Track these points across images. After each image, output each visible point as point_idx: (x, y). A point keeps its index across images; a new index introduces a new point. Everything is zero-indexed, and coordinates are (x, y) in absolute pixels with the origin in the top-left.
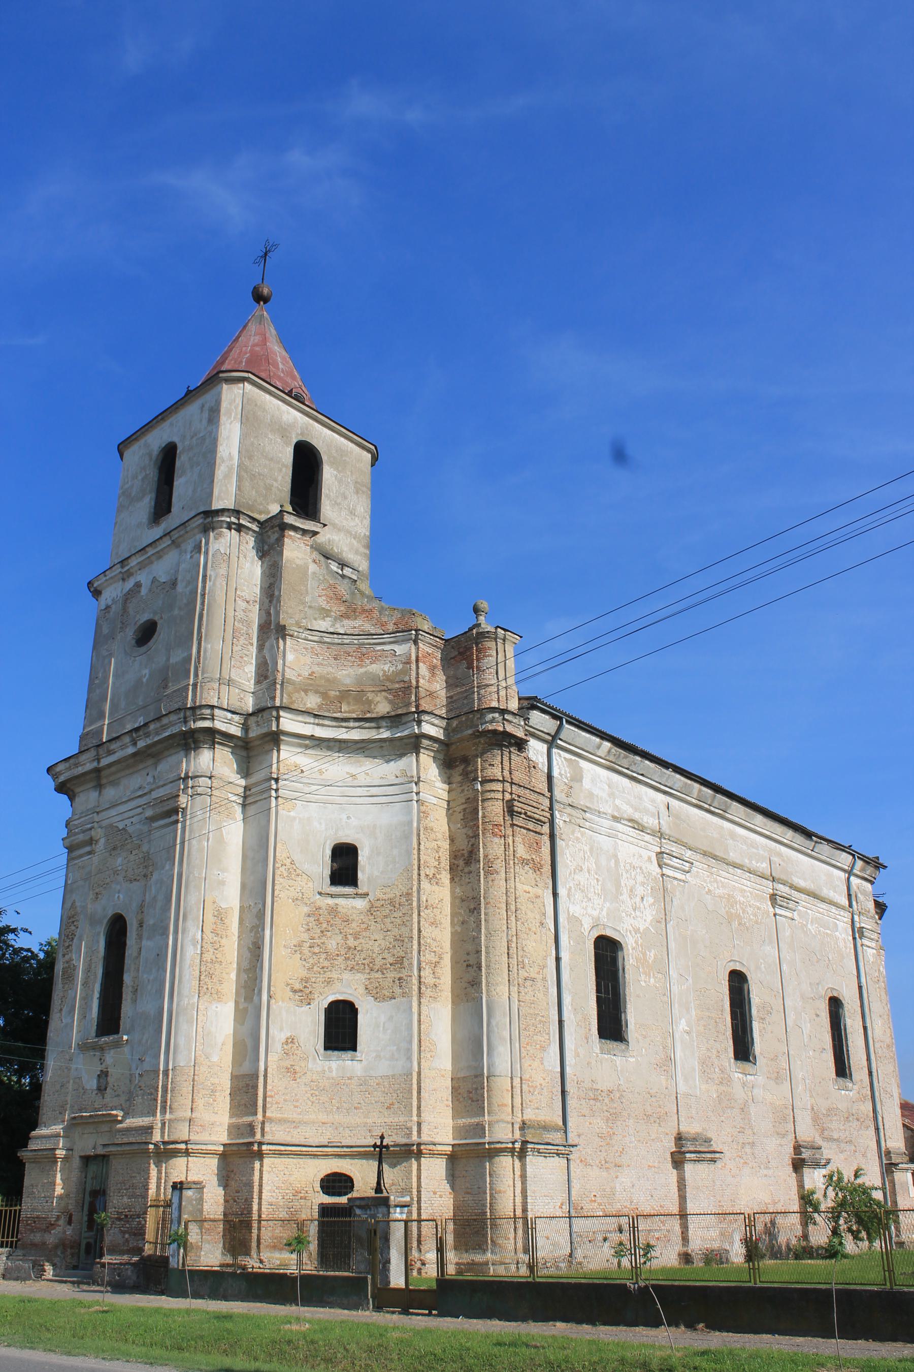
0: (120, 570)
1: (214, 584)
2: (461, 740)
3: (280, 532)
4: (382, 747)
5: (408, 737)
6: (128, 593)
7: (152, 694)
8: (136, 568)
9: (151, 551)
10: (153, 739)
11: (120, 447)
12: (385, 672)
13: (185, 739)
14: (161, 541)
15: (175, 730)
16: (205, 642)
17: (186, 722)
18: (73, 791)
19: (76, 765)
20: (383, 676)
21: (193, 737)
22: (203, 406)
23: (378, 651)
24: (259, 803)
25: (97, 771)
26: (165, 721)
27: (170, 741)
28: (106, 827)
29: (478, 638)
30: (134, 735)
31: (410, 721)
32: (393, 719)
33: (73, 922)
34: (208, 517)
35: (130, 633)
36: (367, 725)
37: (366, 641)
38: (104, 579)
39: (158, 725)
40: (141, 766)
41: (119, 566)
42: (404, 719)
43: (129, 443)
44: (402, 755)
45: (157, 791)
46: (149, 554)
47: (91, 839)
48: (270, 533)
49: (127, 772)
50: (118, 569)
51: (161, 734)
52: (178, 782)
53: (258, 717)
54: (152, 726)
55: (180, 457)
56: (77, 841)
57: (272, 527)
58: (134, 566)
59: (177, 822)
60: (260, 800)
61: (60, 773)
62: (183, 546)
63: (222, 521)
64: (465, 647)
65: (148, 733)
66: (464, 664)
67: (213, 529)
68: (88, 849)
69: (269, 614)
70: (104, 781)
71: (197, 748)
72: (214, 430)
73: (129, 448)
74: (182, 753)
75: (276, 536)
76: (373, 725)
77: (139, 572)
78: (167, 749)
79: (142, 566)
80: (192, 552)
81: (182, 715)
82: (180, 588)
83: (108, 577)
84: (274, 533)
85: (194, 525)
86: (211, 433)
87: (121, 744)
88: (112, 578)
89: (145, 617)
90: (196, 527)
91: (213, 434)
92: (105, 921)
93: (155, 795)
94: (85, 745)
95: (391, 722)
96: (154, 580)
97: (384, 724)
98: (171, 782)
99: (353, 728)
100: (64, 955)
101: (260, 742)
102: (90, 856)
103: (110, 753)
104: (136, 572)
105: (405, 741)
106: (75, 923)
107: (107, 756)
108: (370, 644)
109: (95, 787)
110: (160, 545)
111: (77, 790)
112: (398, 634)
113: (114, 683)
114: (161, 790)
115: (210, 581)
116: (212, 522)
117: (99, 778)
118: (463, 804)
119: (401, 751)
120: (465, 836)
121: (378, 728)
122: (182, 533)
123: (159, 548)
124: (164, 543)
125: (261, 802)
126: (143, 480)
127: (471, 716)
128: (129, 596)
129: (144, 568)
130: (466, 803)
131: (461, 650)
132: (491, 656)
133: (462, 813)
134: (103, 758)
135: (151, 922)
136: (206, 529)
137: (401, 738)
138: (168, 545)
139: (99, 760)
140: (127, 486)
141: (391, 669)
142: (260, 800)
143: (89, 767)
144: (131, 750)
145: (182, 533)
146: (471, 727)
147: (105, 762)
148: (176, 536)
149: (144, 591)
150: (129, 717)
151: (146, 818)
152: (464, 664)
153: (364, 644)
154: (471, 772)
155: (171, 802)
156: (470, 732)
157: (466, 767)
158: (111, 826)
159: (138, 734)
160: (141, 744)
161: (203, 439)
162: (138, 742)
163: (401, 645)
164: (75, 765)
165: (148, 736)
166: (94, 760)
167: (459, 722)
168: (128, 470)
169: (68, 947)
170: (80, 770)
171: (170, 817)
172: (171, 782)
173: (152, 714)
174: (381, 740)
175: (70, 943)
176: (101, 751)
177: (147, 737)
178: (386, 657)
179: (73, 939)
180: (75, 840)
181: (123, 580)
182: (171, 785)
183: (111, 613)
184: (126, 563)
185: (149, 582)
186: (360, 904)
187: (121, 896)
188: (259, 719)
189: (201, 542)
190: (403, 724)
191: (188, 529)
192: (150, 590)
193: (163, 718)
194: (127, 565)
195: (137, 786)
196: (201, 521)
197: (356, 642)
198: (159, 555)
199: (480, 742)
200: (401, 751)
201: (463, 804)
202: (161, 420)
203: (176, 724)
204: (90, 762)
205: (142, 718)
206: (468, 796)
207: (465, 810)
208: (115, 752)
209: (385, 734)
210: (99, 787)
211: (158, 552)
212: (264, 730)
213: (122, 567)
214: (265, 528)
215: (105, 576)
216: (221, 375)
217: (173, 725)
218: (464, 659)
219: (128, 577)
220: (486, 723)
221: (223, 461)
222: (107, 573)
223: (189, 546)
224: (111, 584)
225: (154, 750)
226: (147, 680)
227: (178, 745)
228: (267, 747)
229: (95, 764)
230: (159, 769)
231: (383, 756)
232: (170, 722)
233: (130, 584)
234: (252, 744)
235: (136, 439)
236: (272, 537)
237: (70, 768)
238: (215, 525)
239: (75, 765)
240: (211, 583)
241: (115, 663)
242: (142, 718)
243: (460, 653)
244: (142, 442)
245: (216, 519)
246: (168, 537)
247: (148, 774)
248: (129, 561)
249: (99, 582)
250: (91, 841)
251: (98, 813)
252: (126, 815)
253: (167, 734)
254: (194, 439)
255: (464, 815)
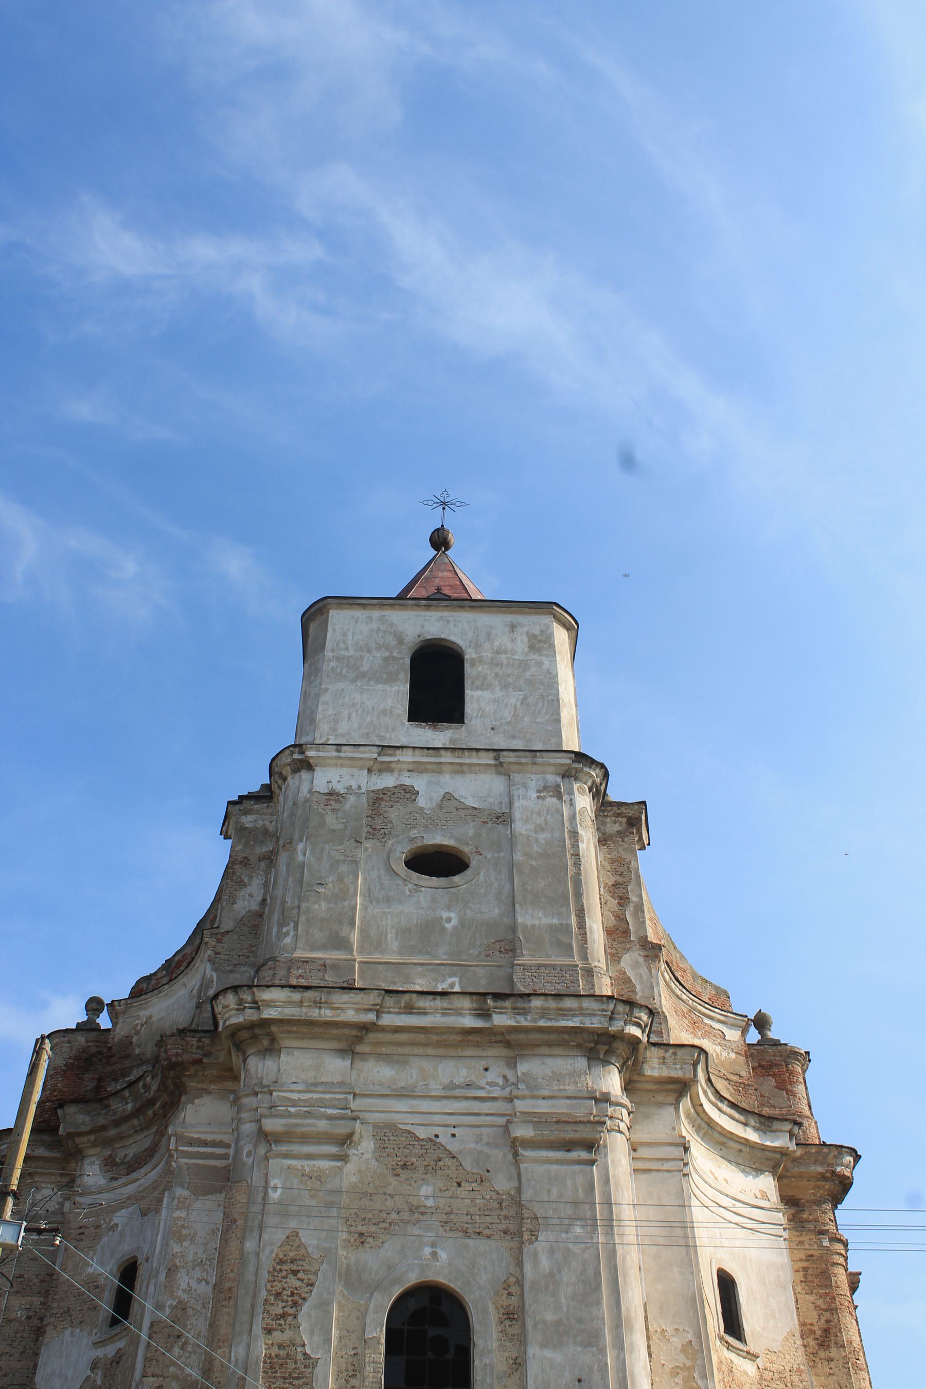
0: (375, 756)
1: (588, 848)
2: (800, 1176)
3: (624, 826)
4: (741, 1151)
5: (774, 1150)
6: (384, 791)
7: (473, 952)
8: (407, 767)
9: (446, 758)
10: (535, 1020)
11: (329, 600)
12: (717, 1054)
13: (597, 1043)
14: (474, 753)
15: (595, 1023)
16: (589, 918)
17: (611, 1019)
18: (273, 1040)
19: (318, 1004)
20: (717, 1058)
21: (610, 1044)
22: (513, 627)
23: (706, 1024)
24: (654, 1174)
25: (366, 1028)
26: (569, 1003)
27: (566, 1037)
28: (376, 1126)
29: (789, 1057)
30: (490, 1002)
31: (782, 1131)
32: (762, 1120)
33: (295, 1272)
34: (579, 762)
35: (401, 851)
36: (736, 1115)
37: (699, 1007)
38: (335, 754)
39: (552, 1004)
40: (469, 1052)
41: (375, 749)
42: (776, 1125)
43: (351, 604)
44: (759, 1171)
45: (529, 1102)
46: (443, 760)
47: (350, 1135)
48: (608, 820)
49: (430, 1051)
50: (372, 754)
51: (556, 1020)
52: (588, 1102)
53: (666, 1051)
54: (536, 1003)
55: (473, 665)
56: (303, 1129)
57: (619, 815)
58: (403, 762)
59: (592, 1162)
60: (658, 1171)
61: (270, 1004)
62: (517, 777)
63: (591, 776)
64: (770, 1061)
65: (523, 1008)
66: (772, 1082)
67: (576, 779)
68: (333, 1149)
69: (621, 919)
70: (359, 1048)
71: (606, 1062)
72: (546, 661)
73: (342, 609)
74: (582, 1063)
75: (617, 827)
76: (742, 1118)
77: (408, 774)
78: (550, 1044)
79: (417, 768)
80: (538, 791)
81: (611, 1006)
82: (520, 827)
83: (342, 755)
84: (615, 822)
85: (552, 761)
86: (540, 664)
87: (445, 1005)
88: (351, 759)
89: (438, 839)
90: (554, 765)
91: (545, 667)
92: (397, 1291)
93: (521, 1106)
94: (300, 976)
95: (761, 1123)
96: (448, 797)
97: (752, 1122)
98: (569, 1098)
99: (725, 1113)
100: (269, 1331)
101: (653, 1087)
102: (339, 1164)
103: (410, 1010)
104: (401, 770)
105: (768, 1153)
106: (301, 1275)
107: (400, 1013)
108: (700, 1012)
109: (342, 1052)
110: (469, 757)
111: (286, 1043)
112: (729, 1014)
113: (365, 908)
114: (541, 1102)
115: (583, 842)
116: (581, 770)
117: (359, 1040)
118: (801, 1260)
119: (757, 1165)
120: (813, 1306)
121: (745, 1124)
122: (524, 760)
123: (467, 761)
124: (480, 758)
125: (660, 1174)
126: (385, 659)
127: (825, 1150)
128: (378, 798)
129: (421, 773)
130: (807, 1260)
131: (763, 1063)
132: (801, 1083)
133: (801, 1274)
134: (389, 1013)
135: (550, 1317)
136: (568, 774)
137: (764, 1148)
138: (487, 765)
139: (379, 1013)
140: (343, 653)
141: (725, 1054)
142: (658, 1171)
143: (350, 1016)
144: (469, 1022)
145: (524, 760)
146: (822, 1164)
147: (387, 1020)
148: (512, 760)
149: (421, 802)
150: (419, 969)
151: (516, 1138)
152: (772, 1082)
153: (695, 1009)
154: (807, 1221)
155: (588, 1128)
156: (820, 1169)
157: (798, 1212)
158: (393, 1128)
159: (500, 1003)
160: (501, 1020)
161: (524, 665)
162: (495, 1016)
163: (730, 1029)
164: (315, 1002)
165: (525, 1014)
166: (370, 1010)
167: (806, 1153)
168: (345, 635)
169: (284, 1316)
170: (327, 1014)
171: (568, 1151)
172: (569, 1098)
173: (483, 982)
174: (746, 1142)
175: (292, 1311)
176: (390, 1001)
177: (518, 1014)
178: (714, 1036)
179: (295, 1304)
180: (297, 1125)
181: (370, 770)
182: (568, 1101)
183: (347, 806)
184: (390, 751)
185: (438, 794)
186: (748, 1367)
187: (443, 1255)
188: (668, 1055)
189: (558, 786)
190: (772, 1131)
191: (539, 760)
192: (441, 807)
193: (566, 999)
194: (390, 755)
195: (458, 1080)
196: (569, 761)
197: (690, 1001)
198: (459, 770)
199: (824, 1186)
200: (757, 1165)
201: (801, 1260)
202: (425, 606)
203: (594, 1015)
204: (357, 1010)
205: (456, 980)
206: (811, 1252)
207: (805, 1269)
208: (425, 1014)
209: (752, 1136)
210: (349, 1051)
211: (460, 764)
212: (677, 1073)
213: (379, 755)
214: (604, 811)
215: (340, 751)
216: (555, 607)
217: (584, 1015)
218: (769, 1075)
219: (380, 771)
220: (842, 1165)
221: (565, 705)
222: (344, 748)
223: (534, 782)
224: (342, 766)
225: (522, 1037)
226: (455, 928)
227: (579, 1046)
228: (660, 1098)
229: (371, 1017)
230: (523, 1067)
231: (738, 1164)
232: (581, 1009)
233: (388, 781)
234: (638, 1085)
235: (364, 606)
236: (608, 825)
237: (300, 1004)
238: (581, 775)
239: (315, 1002)
240: (584, 846)
241: (365, 879)
242: (456, 980)
243: (760, 1066)
244: (376, 614)
245: (587, 769)
246: (491, 755)
247: (486, 1070)
248: (398, 752)
249: (321, 754)
250: (346, 1140)
251: (355, 1095)
252: (438, 1119)
253: (570, 1024)
254: (503, 657)
255: (805, 1276)
